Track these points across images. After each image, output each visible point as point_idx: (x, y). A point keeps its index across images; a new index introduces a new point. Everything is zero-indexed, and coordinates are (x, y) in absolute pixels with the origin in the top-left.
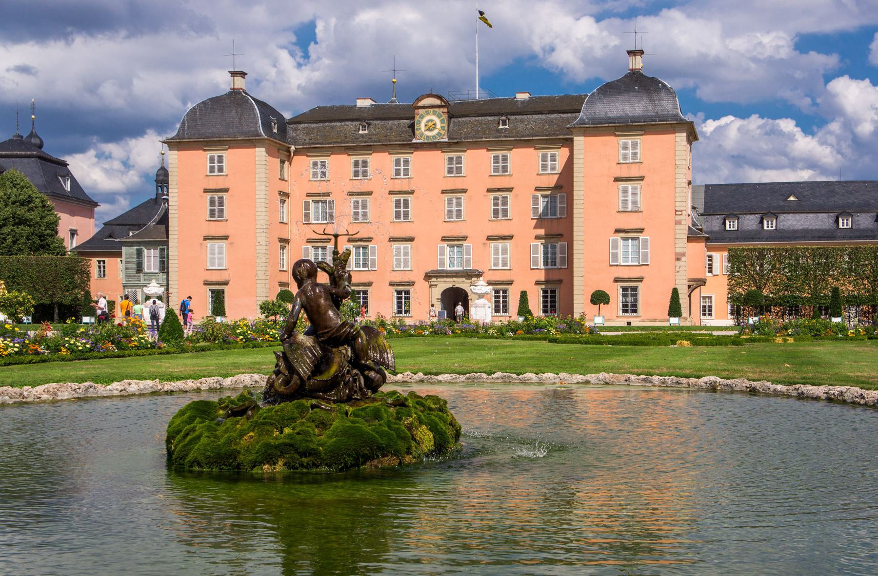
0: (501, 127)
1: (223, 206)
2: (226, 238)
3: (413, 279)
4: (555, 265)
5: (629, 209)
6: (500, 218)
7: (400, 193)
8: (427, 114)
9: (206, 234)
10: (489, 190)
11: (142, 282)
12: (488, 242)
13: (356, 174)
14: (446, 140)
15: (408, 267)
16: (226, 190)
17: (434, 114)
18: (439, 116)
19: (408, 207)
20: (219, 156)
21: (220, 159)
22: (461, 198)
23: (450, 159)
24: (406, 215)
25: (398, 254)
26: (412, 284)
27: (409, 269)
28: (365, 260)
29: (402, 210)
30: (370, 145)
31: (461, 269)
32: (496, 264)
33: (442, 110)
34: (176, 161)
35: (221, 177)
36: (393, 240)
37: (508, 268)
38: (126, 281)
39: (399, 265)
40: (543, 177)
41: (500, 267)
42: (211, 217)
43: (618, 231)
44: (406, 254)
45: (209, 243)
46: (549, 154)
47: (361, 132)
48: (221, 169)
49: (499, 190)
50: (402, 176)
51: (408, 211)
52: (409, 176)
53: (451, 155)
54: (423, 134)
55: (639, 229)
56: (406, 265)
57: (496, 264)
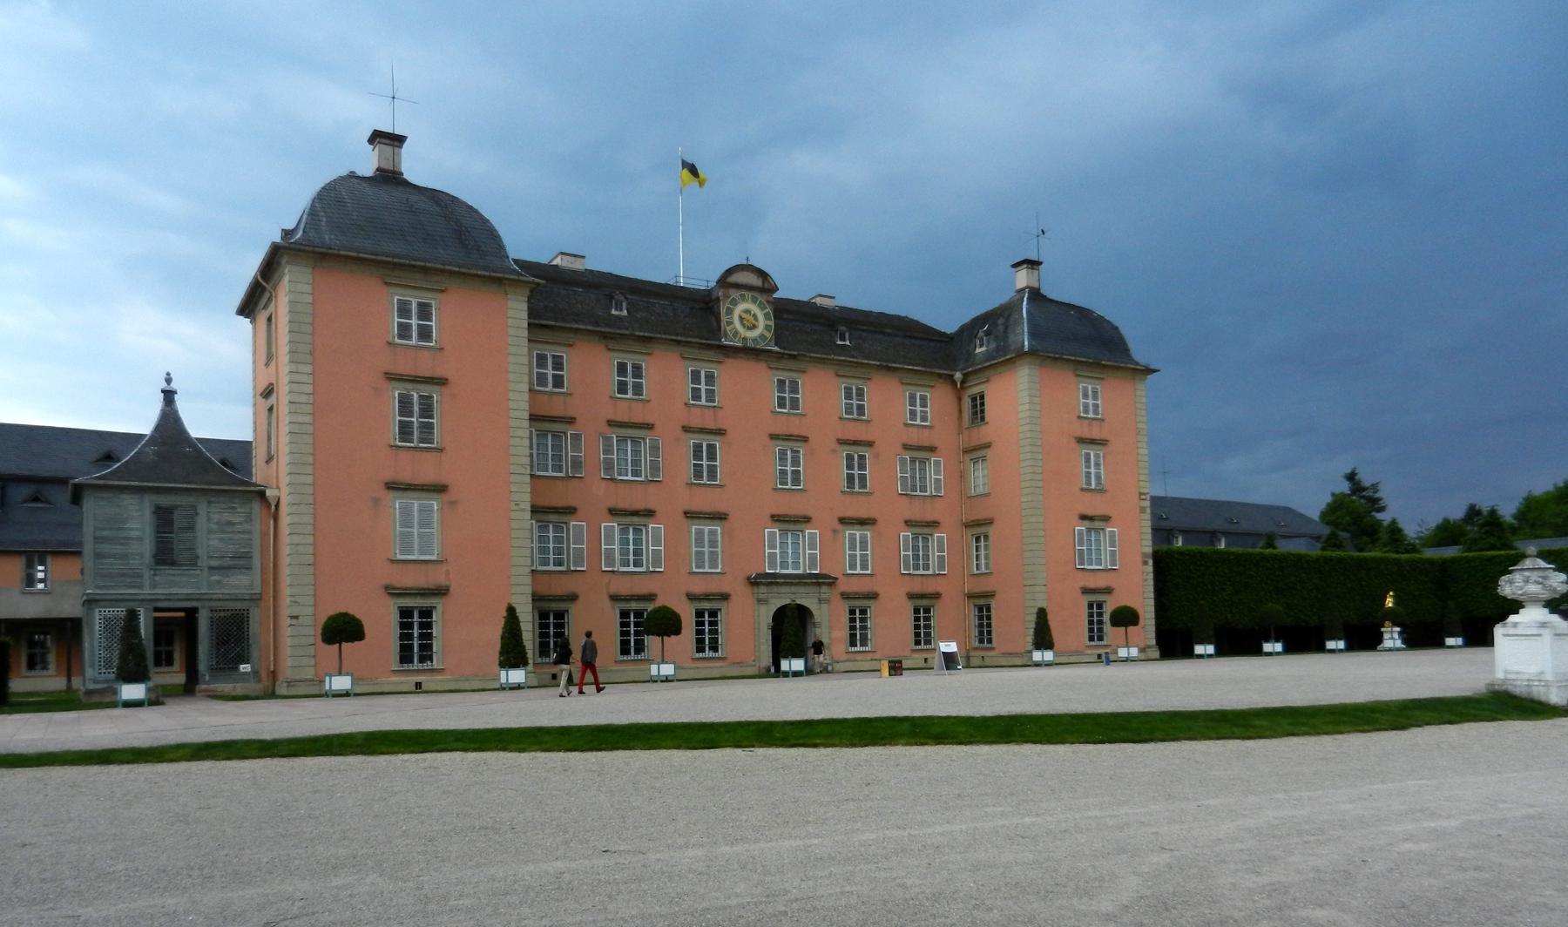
0: (839, 343)
1: (432, 417)
2: (440, 489)
3: (725, 589)
4: (928, 569)
5: (1093, 487)
6: (857, 489)
7: (702, 431)
8: (743, 300)
9: (389, 475)
10: (841, 442)
11: (146, 591)
12: (840, 527)
13: (622, 388)
14: (776, 349)
15: (717, 568)
16: (442, 382)
17: (754, 300)
18: (762, 308)
19: (714, 459)
20: (420, 305)
21: (424, 311)
22: (799, 452)
23: (781, 383)
24: (712, 473)
25: (699, 542)
26: (725, 597)
27: (719, 570)
28: (637, 553)
29: (705, 463)
30: (651, 338)
31: (800, 571)
32: (853, 566)
33: (765, 296)
34: (309, 299)
35: (426, 353)
36: (690, 515)
37: (869, 572)
38: (98, 587)
39: (700, 564)
40: (911, 429)
41: (858, 571)
42: (402, 440)
43: (1084, 517)
44: (713, 544)
45: (397, 502)
46: (918, 394)
47: (613, 312)
48: (425, 334)
49: (855, 443)
50: (703, 402)
51: (715, 466)
52: (716, 404)
53: (782, 375)
54: (736, 332)
55: (1104, 516)
56: (713, 564)
57: (853, 566)
